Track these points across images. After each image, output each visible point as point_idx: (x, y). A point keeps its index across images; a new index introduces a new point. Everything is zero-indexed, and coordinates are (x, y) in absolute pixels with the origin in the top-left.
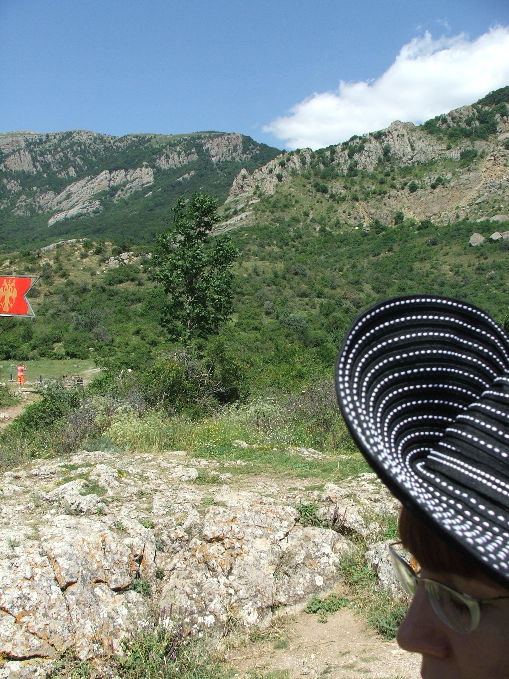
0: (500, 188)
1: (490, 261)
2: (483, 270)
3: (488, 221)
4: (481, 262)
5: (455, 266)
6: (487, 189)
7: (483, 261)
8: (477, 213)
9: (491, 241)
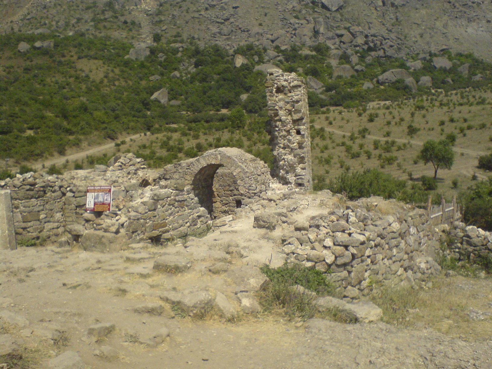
0: (45, 8)
1: (34, 63)
2: (30, 70)
3: (33, 33)
4: (27, 64)
5: (7, 68)
6: (35, 8)
7: (28, 63)
8: (28, 27)
9: (35, 48)
